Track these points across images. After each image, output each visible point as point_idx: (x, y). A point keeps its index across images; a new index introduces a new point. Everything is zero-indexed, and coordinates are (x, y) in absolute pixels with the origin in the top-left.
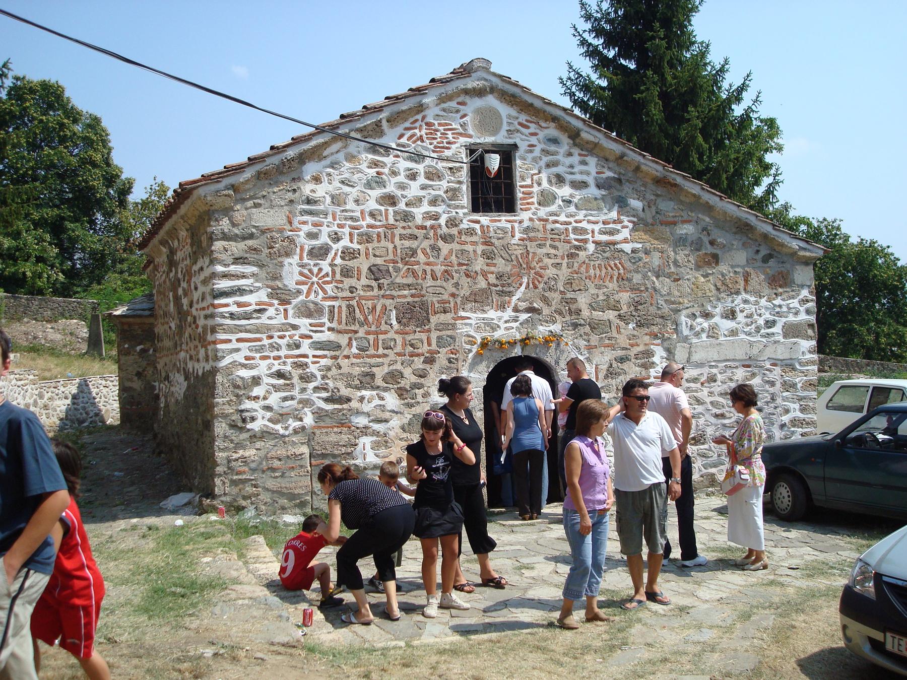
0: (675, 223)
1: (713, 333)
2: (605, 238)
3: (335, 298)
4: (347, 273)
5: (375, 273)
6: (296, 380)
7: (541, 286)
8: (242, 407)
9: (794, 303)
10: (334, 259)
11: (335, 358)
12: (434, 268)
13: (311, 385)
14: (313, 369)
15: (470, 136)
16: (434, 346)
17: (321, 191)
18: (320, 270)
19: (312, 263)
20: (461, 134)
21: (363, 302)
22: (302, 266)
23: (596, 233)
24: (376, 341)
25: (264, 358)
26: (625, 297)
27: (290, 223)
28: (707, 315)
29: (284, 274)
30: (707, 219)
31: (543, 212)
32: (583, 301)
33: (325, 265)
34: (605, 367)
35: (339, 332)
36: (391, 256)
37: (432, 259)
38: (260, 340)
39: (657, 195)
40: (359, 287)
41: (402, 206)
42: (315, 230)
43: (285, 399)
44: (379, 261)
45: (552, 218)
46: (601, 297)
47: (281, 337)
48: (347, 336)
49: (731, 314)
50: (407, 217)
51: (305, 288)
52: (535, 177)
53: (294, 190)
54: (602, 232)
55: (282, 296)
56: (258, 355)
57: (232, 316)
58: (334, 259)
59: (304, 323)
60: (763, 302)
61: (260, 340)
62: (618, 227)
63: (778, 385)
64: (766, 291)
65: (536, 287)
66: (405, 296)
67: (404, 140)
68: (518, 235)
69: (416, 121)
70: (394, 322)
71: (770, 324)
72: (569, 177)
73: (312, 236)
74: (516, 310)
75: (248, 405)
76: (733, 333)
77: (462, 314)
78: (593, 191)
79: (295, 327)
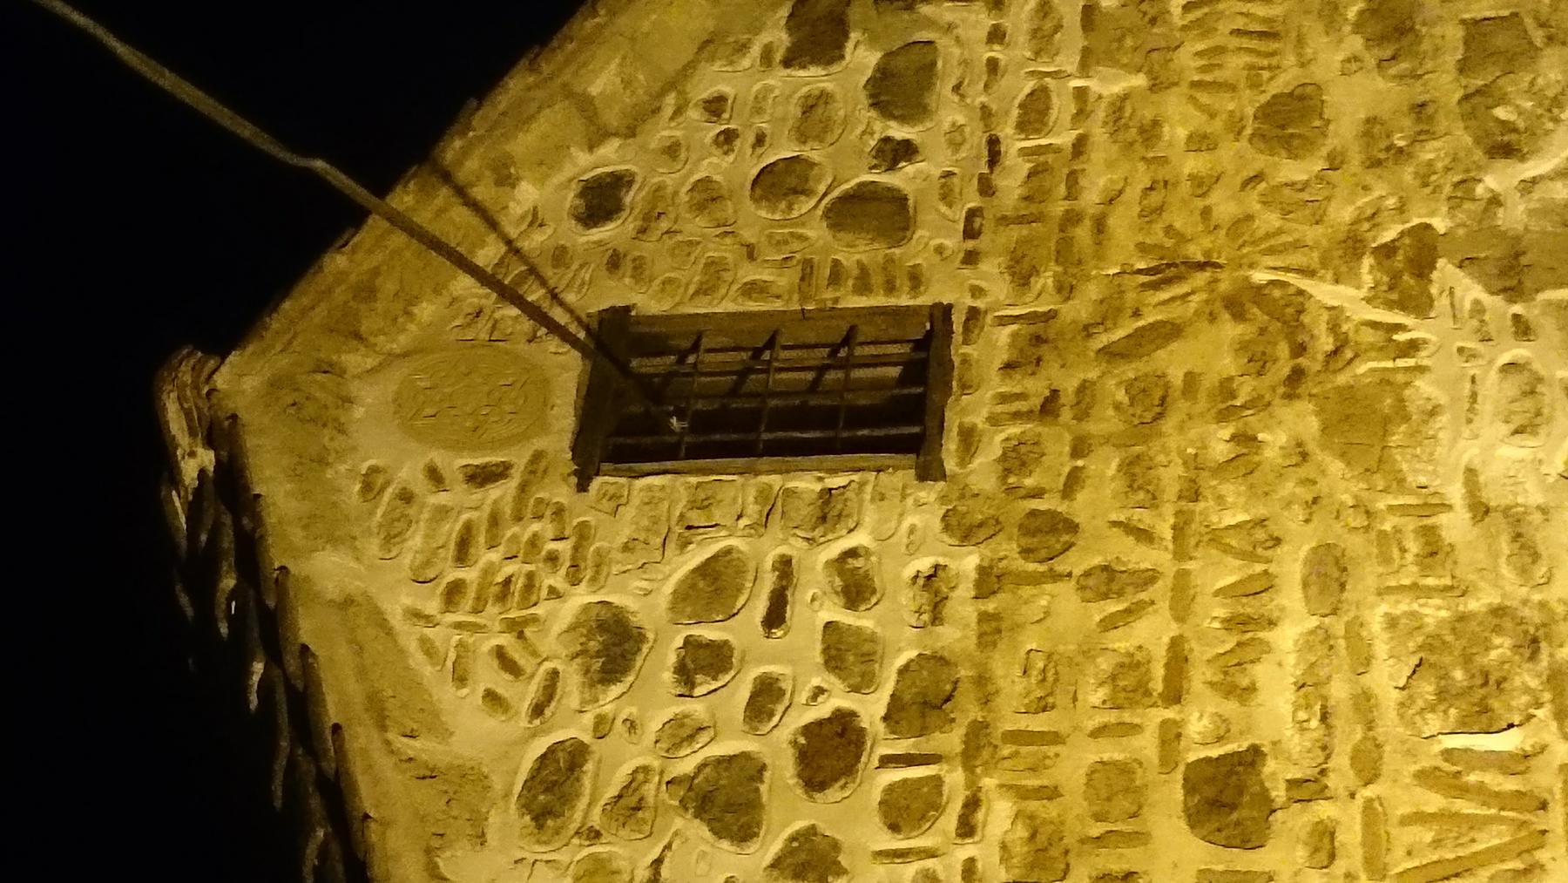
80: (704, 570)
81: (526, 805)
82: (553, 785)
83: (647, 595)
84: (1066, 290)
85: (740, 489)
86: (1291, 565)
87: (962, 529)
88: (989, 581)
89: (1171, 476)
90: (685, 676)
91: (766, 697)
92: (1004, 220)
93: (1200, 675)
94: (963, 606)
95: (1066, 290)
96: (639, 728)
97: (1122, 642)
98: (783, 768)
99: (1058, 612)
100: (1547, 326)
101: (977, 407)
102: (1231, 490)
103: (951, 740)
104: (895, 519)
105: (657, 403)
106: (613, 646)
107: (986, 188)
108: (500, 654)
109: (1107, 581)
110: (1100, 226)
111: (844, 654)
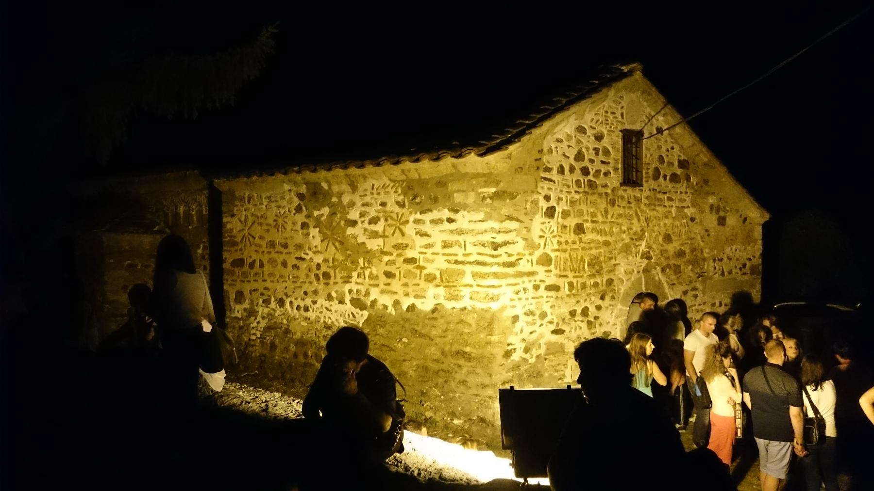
8: (509, 341)
14: (546, 308)
16: (604, 288)
25: (520, 299)
28: (721, 260)
33: (553, 223)
43: (531, 333)
51: (542, 242)
56: (516, 297)
59: (541, 270)
80: (609, 151)
81: (580, 126)
82: (581, 130)
83: (606, 142)
84: (645, 204)
85: (619, 156)
86: (608, 238)
87: (613, 190)
88: (607, 194)
89: (620, 221)
90: (595, 149)
93: (594, 225)
94: (603, 190)
95: (645, 204)
96: (588, 142)
97: (599, 214)
98: (583, 164)
99: (603, 204)
100: (638, 276)
101: (630, 192)
102: (618, 230)
103: (587, 190)
104: (615, 179)
105: (631, 139)
106: (599, 138)
107: (660, 192)
109: (606, 212)
110: (654, 210)
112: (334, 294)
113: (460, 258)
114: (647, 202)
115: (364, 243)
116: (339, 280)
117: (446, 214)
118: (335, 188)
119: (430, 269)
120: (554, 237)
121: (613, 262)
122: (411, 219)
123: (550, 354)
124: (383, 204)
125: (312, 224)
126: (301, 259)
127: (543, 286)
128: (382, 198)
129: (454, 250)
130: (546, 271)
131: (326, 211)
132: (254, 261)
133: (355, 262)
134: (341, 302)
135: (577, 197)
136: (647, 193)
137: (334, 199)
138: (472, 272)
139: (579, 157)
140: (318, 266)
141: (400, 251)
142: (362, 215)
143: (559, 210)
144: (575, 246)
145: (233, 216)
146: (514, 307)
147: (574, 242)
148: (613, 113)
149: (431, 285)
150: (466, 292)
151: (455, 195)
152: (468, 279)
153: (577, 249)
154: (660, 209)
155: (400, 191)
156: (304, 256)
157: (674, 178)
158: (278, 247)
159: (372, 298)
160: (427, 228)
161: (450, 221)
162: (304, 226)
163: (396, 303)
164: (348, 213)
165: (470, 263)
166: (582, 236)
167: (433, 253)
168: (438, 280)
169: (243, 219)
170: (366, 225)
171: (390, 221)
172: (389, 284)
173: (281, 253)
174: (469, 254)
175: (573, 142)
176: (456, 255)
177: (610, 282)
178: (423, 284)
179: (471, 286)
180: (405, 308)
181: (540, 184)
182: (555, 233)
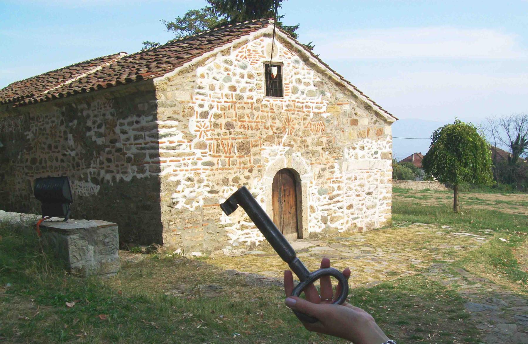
0: (342, 105)
1: (356, 157)
2: (317, 111)
3: (212, 139)
4: (216, 125)
5: (229, 126)
6: (195, 182)
7: (293, 134)
9: (385, 143)
10: (210, 119)
11: (212, 170)
12: (252, 124)
13: (203, 184)
14: (203, 176)
15: (265, 58)
16: (252, 164)
17: (205, 82)
18: (205, 124)
19: (202, 120)
20: (262, 57)
21: (224, 141)
22: (198, 122)
23: (314, 108)
24: (229, 161)
25: (181, 170)
26: (324, 140)
27: (192, 99)
28: (354, 148)
29: (189, 126)
30: (354, 103)
31: (294, 97)
32: (309, 140)
33: (207, 121)
34: (317, 173)
35: (214, 156)
36: (234, 118)
37: (251, 120)
38: (179, 161)
39: (336, 91)
40: (221, 133)
41: (238, 92)
42: (202, 103)
43: (191, 192)
44: (229, 120)
45: (297, 100)
46: (316, 140)
47: (189, 159)
48: (217, 159)
49: (363, 148)
50: (240, 98)
51: (199, 133)
52: (290, 79)
53: (194, 81)
54: (316, 108)
55: (189, 137)
56: (178, 169)
57: (167, 148)
58: (210, 119)
59: (198, 152)
60: (374, 142)
61: (179, 161)
62: (322, 105)
63: (379, 181)
64: (375, 137)
65: (291, 134)
66: (240, 138)
67: (238, 58)
68: (285, 108)
69: (243, 48)
70: (236, 151)
71: (376, 153)
72: (303, 80)
73: (201, 106)
74: (284, 145)
75: (175, 195)
76: (363, 157)
77: (263, 147)
78: (312, 88)
79: (194, 154)
91: (238, 82)
92: (294, 104)
108: (242, 56)
111: (243, 90)
112: (82, 176)
113: (143, 146)
114: (287, 108)
115: (95, 141)
116: (85, 167)
117: (135, 118)
118: (79, 107)
119: (129, 154)
120: (207, 131)
121: (259, 148)
122: (118, 123)
123: (206, 206)
124: (104, 115)
125: (68, 130)
126: (64, 155)
127: (200, 162)
128: (102, 111)
129: (140, 141)
130: (202, 153)
131: (75, 122)
132: (42, 159)
133: (92, 154)
134: (87, 181)
135: (227, 105)
136: (288, 103)
137: (79, 114)
138: (149, 154)
139: (228, 79)
140: (74, 158)
141: (113, 144)
142: (94, 123)
143: (212, 112)
144: (226, 137)
145: (29, 131)
146: (176, 175)
147: (226, 134)
148: (253, 51)
149: (129, 165)
150: (147, 167)
151: (139, 106)
152: (147, 159)
153: (227, 139)
154: (300, 113)
155: (111, 105)
156: (66, 153)
157: (311, 94)
158: (53, 149)
159: (101, 176)
160: (126, 128)
161: (137, 122)
162: (65, 132)
163: (114, 178)
164: (86, 123)
165: (148, 149)
166: (232, 130)
167: (130, 144)
168: (133, 161)
169: (34, 131)
170: (96, 130)
171: (108, 126)
172: (109, 167)
173: (54, 152)
174: (148, 143)
175: (222, 70)
176: (141, 144)
177: (257, 161)
178: (126, 164)
179: (148, 163)
180: (118, 181)
181: (195, 97)
182: (209, 129)
